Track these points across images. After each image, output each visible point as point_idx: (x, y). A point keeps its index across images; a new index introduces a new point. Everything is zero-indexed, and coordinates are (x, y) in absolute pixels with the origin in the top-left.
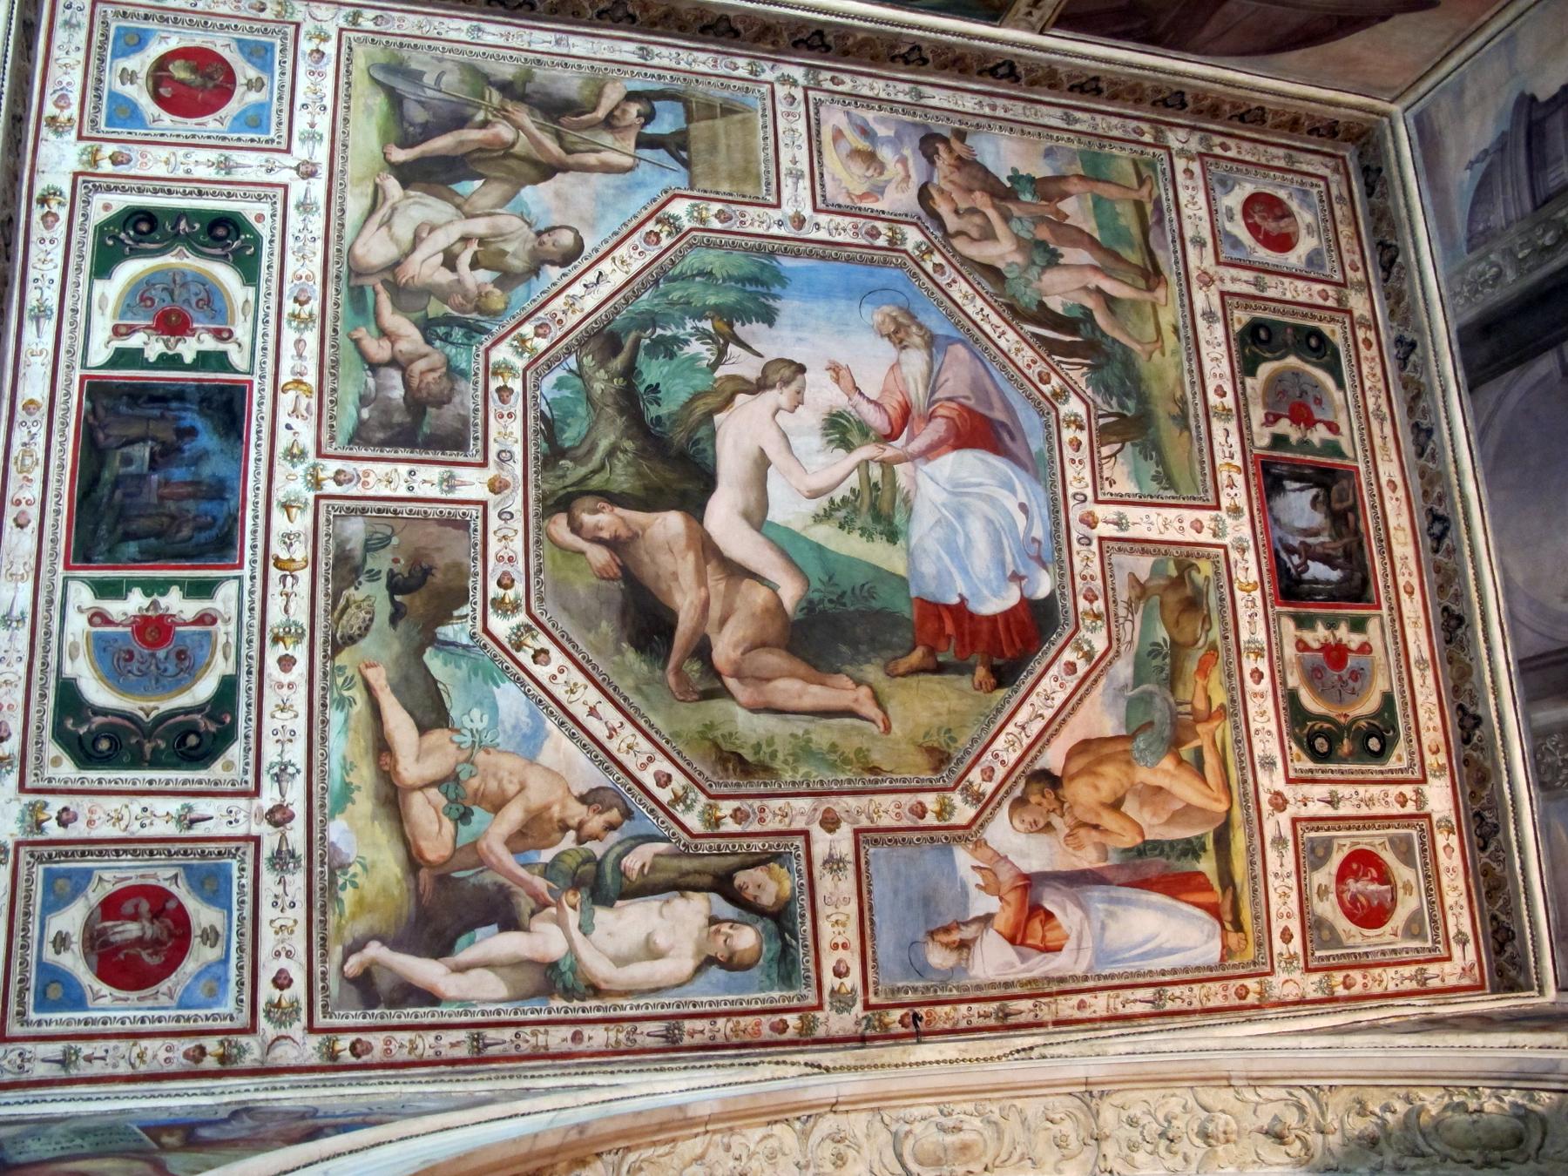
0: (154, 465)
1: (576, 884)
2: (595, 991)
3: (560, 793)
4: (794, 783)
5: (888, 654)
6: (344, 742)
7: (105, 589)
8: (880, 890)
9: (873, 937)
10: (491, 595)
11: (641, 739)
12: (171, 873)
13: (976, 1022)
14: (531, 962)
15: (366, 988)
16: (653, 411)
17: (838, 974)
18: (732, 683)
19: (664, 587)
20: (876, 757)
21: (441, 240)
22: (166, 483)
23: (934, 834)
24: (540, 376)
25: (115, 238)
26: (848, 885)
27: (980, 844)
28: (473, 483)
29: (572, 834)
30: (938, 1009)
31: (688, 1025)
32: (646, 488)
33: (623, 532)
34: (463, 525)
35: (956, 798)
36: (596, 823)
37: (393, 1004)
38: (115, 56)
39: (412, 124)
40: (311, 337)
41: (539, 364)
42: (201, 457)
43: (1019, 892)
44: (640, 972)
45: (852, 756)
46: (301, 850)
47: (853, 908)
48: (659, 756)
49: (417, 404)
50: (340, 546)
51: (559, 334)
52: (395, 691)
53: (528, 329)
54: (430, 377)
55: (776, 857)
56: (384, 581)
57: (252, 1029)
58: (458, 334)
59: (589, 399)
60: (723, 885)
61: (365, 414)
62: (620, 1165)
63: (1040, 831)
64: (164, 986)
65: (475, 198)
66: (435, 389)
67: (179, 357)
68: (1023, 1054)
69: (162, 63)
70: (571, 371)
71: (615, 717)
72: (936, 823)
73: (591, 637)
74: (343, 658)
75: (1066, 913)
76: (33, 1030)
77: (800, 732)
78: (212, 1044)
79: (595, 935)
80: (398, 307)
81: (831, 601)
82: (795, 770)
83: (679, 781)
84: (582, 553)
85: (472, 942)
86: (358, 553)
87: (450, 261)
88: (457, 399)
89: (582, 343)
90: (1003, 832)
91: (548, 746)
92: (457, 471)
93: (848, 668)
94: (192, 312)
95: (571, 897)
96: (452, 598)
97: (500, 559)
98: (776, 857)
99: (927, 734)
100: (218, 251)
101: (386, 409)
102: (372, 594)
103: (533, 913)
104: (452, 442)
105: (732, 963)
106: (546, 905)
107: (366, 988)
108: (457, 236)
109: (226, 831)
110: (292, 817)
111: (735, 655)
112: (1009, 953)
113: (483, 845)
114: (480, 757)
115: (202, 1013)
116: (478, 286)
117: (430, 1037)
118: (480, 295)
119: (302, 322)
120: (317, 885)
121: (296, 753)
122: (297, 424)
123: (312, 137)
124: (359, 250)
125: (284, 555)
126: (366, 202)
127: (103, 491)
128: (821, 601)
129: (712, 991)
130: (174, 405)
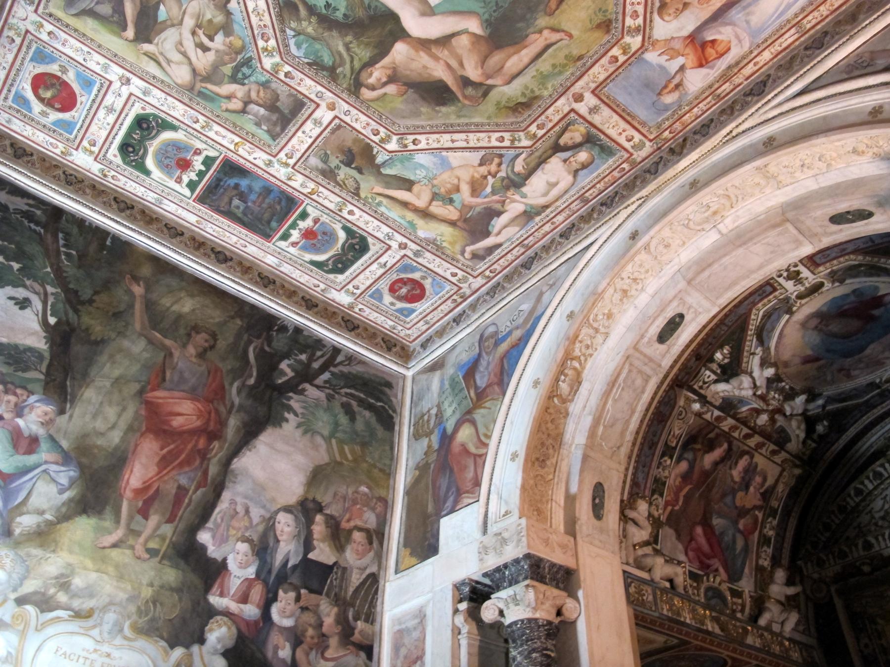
0: (245, 202)
1: (507, 188)
2: (547, 207)
3: (471, 170)
4: (550, 96)
5: (542, 7)
6: (394, 213)
7: (285, 237)
8: (622, 98)
9: (633, 117)
10: (377, 141)
11: (478, 135)
12: (395, 275)
13: (705, 108)
14: (517, 217)
15: (477, 257)
16: (339, 15)
17: (629, 140)
18: (490, 82)
19: (426, 75)
20: (576, 52)
21: (189, 44)
22: (254, 202)
23: (629, 62)
24: (288, 52)
25: (132, 161)
26: (606, 111)
27: (654, 43)
28: (324, 115)
29: (489, 177)
30: (684, 118)
31: (587, 195)
32: (375, 47)
33: (389, 72)
34: (339, 127)
35: (628, 39)
36: (493, 168)
37: (490, 255)
38: (30, 112)
39: (112, 16)
40: (216, 127)
41: (283, 50)
42: (250, 189)
43: (690, 46)
44: (555, 192)
45: (565, 62)
46: (419, 248)
47: (616, 117)
48: (491, 134)
49: (272, 107)
50: (317, 169)
51: (272, 31)
52: (388, 188)
53: (261, 43)
54: (262, 94)
55: (568, 125)
56: (342, 166)
57: (460, 288)
58: (245, 70)
59: (314, 39)
60: (557, 148)
61: (265, 128)
62: (589, 323)
63: (682, 11)
64: (427, 293)
65: (170, 14)
66: (268, 96)
67: (200, 171)
68: (728, 137)
69: (41, 100)
70: (294, 36)
71: (463, 136)
72: (626, 58)
73: (423, 117)
74: (363, 195)
75: (722, 34)
76: (411, 324)
77: (535, 73)
78: (455, 297)
79: (529, 195)
80: (219, 83)
81: (494, 11)
82: (546, 88)
83: (507, 135)
84: (385, 94)
85: (493, 226)
86: (325, 166)
87: (206, 49)
88: (279, 92)
89: (282, 20)
90: (662, 29)
91: (451, 160)
92: (314, 116)
93: (531, 30)
94: (182, 155)
95: (509, 194)
96: (367, 152)
97: (364, 128)
98: (568, 125)
99: (591, 20)
100: (154, 132)
101: (268, 120)
102: (344, 173)
103: (503, 206)
104: (299, 104)
105: (584, 166)
106: (504, 202)
107: (475, 256)
108: (190, 36)
109: (395, 260)
110: (406, 244)
111: (480, 71)
112: (704, 71)
113: (466, 203)
114: (435, 182)
115: (444, 292)
116: (224, 44)
117: (509, 255)
118: (230, 47)
119: (207, 126)
120: (434, 251)
121: (386, 229)
122: (255, 155)
123: (106, 68)
124: (179, 81)
125: (310, 190)
126: (152, 63)
127: (245, 219)
128: (491, 15)
129: (586, 179)
130: (222, 183)
